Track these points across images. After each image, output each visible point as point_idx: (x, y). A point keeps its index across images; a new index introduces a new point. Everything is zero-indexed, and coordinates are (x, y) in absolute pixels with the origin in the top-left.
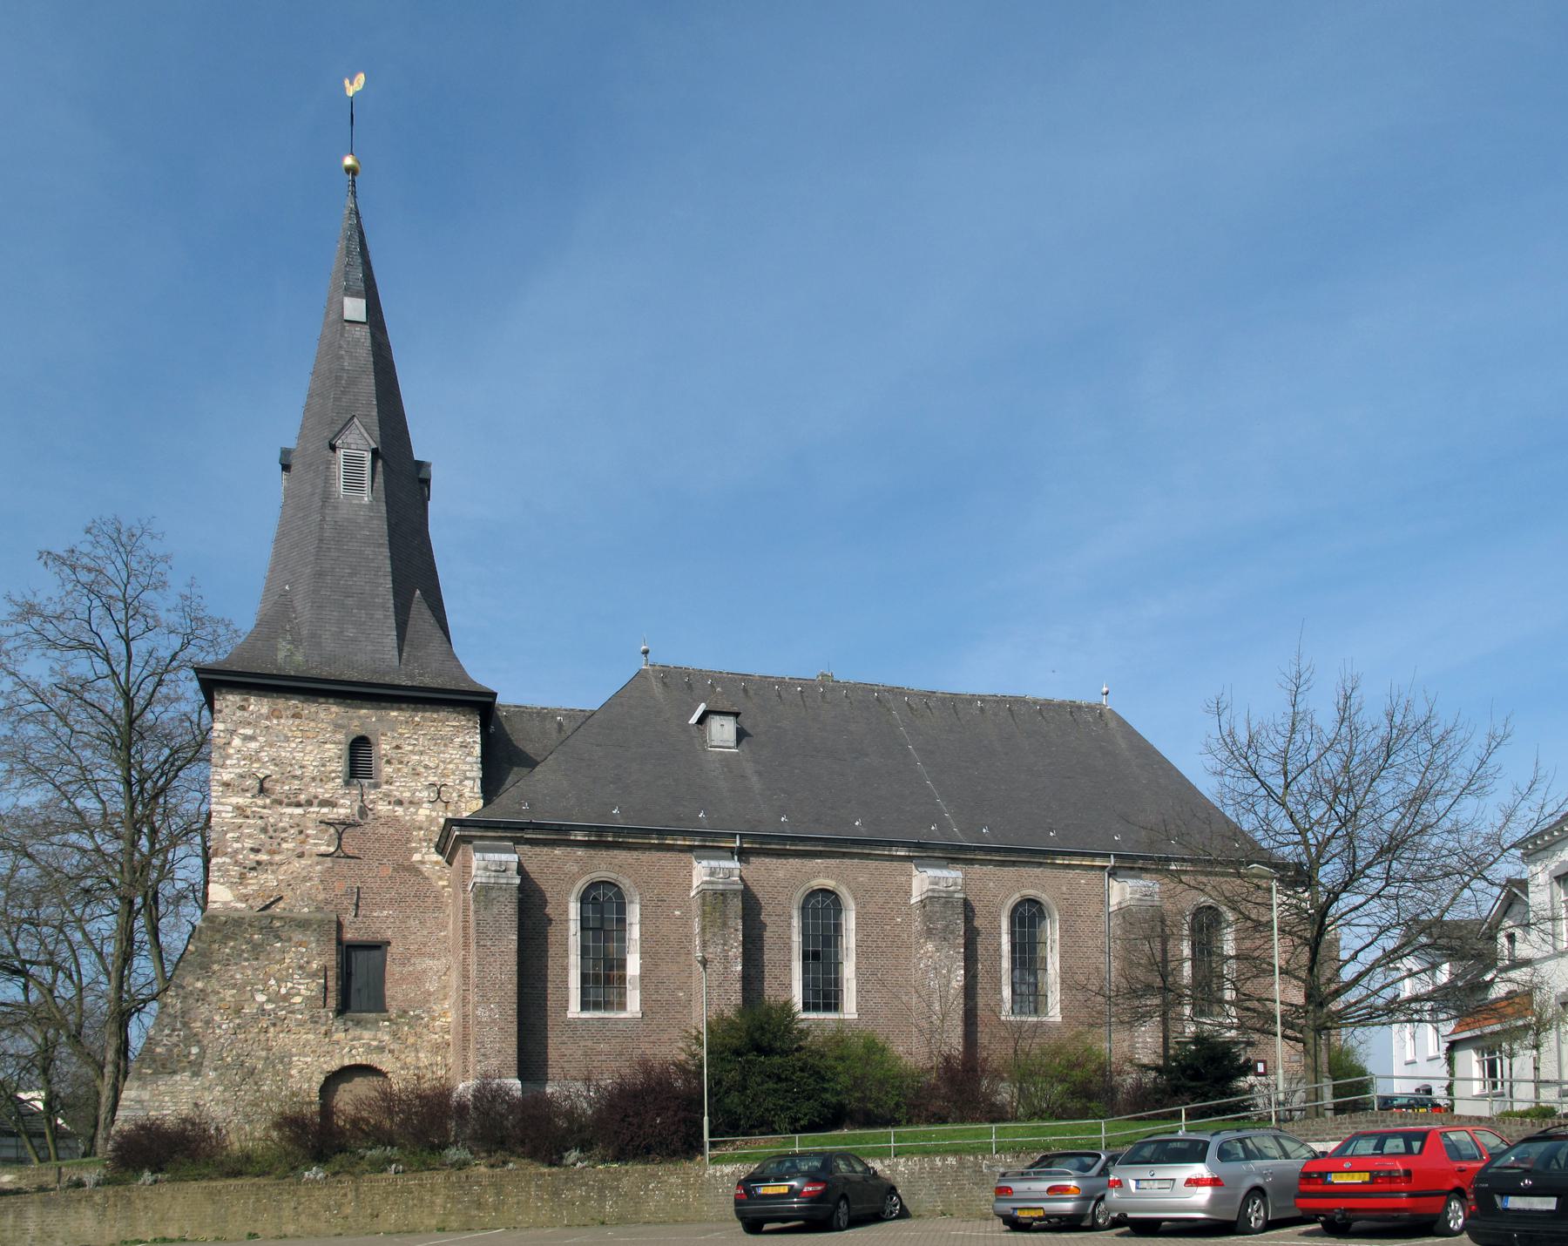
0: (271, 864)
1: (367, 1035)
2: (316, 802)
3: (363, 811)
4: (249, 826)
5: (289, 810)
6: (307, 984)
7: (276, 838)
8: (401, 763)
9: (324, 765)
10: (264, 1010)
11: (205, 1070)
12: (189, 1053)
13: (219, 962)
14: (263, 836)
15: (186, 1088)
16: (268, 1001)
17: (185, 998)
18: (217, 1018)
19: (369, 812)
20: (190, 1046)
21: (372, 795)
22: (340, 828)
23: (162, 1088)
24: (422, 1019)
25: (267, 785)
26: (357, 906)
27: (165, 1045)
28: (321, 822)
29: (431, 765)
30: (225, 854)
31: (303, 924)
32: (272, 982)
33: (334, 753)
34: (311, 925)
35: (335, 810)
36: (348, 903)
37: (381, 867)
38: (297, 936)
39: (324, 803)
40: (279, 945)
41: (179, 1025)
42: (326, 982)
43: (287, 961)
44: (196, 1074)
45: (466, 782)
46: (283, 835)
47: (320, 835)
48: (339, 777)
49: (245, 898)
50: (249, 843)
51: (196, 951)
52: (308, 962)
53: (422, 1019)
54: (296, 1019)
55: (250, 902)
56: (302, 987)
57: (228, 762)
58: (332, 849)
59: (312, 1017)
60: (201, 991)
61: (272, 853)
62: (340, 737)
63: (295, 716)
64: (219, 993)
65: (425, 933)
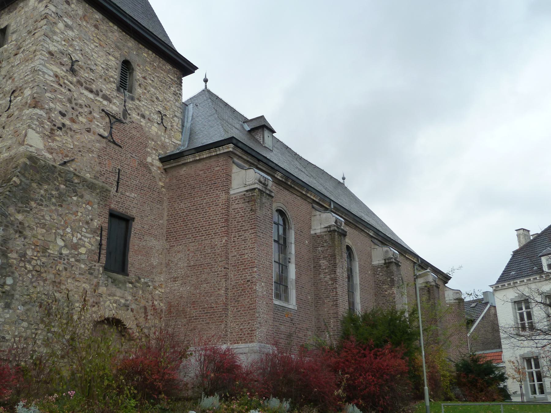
0: (71, 129)
1: (119, 292)
2: (101, 94)
3: (125, 113)
4: (61, 94)
5: (86, 93)
6: (90, 238)
7: (77, 110)
8: (146, 89)
9: (107, 70)
10: (61, 254)
11: (15, 304)
12: (5, 283)
13: (35, 200)
14: (68, 105)
16: (65, 246)
17: (7, 226)
18: (29, 253)
19: (128, 115)
20: (6, 276)
21: (130, 104)
22: (113, 120)
25: (75, 67)
26: (118, 183)
28: (103, 110)
29: (160, 98)
30: (42, 108)
31: (91, 187)
32: (68, 230)
33: (114, 63)
34: (95, 189)
35: (111, 105)
36: (113, 179)
38: (87, 197)
39: (105, 97)
40: (75, 198)
42: (101, 240)
43: (79, 214)
45: (175, 118)
46: (80, 110)
48: (114, 82)
49: (50, 150)
50: (59, 107)
51: (20, 184)
52: (92, 220)
53: (149, 286)
54: (80, 268)
55: (54, 155)
56: (86, 240)
57: (55, 37)
58: (106, 134)
59: (91, 268)
60: (20, 223)
61: (73, 121)
62: (117, 54)
63: (96, 27)
64: (34, 229)
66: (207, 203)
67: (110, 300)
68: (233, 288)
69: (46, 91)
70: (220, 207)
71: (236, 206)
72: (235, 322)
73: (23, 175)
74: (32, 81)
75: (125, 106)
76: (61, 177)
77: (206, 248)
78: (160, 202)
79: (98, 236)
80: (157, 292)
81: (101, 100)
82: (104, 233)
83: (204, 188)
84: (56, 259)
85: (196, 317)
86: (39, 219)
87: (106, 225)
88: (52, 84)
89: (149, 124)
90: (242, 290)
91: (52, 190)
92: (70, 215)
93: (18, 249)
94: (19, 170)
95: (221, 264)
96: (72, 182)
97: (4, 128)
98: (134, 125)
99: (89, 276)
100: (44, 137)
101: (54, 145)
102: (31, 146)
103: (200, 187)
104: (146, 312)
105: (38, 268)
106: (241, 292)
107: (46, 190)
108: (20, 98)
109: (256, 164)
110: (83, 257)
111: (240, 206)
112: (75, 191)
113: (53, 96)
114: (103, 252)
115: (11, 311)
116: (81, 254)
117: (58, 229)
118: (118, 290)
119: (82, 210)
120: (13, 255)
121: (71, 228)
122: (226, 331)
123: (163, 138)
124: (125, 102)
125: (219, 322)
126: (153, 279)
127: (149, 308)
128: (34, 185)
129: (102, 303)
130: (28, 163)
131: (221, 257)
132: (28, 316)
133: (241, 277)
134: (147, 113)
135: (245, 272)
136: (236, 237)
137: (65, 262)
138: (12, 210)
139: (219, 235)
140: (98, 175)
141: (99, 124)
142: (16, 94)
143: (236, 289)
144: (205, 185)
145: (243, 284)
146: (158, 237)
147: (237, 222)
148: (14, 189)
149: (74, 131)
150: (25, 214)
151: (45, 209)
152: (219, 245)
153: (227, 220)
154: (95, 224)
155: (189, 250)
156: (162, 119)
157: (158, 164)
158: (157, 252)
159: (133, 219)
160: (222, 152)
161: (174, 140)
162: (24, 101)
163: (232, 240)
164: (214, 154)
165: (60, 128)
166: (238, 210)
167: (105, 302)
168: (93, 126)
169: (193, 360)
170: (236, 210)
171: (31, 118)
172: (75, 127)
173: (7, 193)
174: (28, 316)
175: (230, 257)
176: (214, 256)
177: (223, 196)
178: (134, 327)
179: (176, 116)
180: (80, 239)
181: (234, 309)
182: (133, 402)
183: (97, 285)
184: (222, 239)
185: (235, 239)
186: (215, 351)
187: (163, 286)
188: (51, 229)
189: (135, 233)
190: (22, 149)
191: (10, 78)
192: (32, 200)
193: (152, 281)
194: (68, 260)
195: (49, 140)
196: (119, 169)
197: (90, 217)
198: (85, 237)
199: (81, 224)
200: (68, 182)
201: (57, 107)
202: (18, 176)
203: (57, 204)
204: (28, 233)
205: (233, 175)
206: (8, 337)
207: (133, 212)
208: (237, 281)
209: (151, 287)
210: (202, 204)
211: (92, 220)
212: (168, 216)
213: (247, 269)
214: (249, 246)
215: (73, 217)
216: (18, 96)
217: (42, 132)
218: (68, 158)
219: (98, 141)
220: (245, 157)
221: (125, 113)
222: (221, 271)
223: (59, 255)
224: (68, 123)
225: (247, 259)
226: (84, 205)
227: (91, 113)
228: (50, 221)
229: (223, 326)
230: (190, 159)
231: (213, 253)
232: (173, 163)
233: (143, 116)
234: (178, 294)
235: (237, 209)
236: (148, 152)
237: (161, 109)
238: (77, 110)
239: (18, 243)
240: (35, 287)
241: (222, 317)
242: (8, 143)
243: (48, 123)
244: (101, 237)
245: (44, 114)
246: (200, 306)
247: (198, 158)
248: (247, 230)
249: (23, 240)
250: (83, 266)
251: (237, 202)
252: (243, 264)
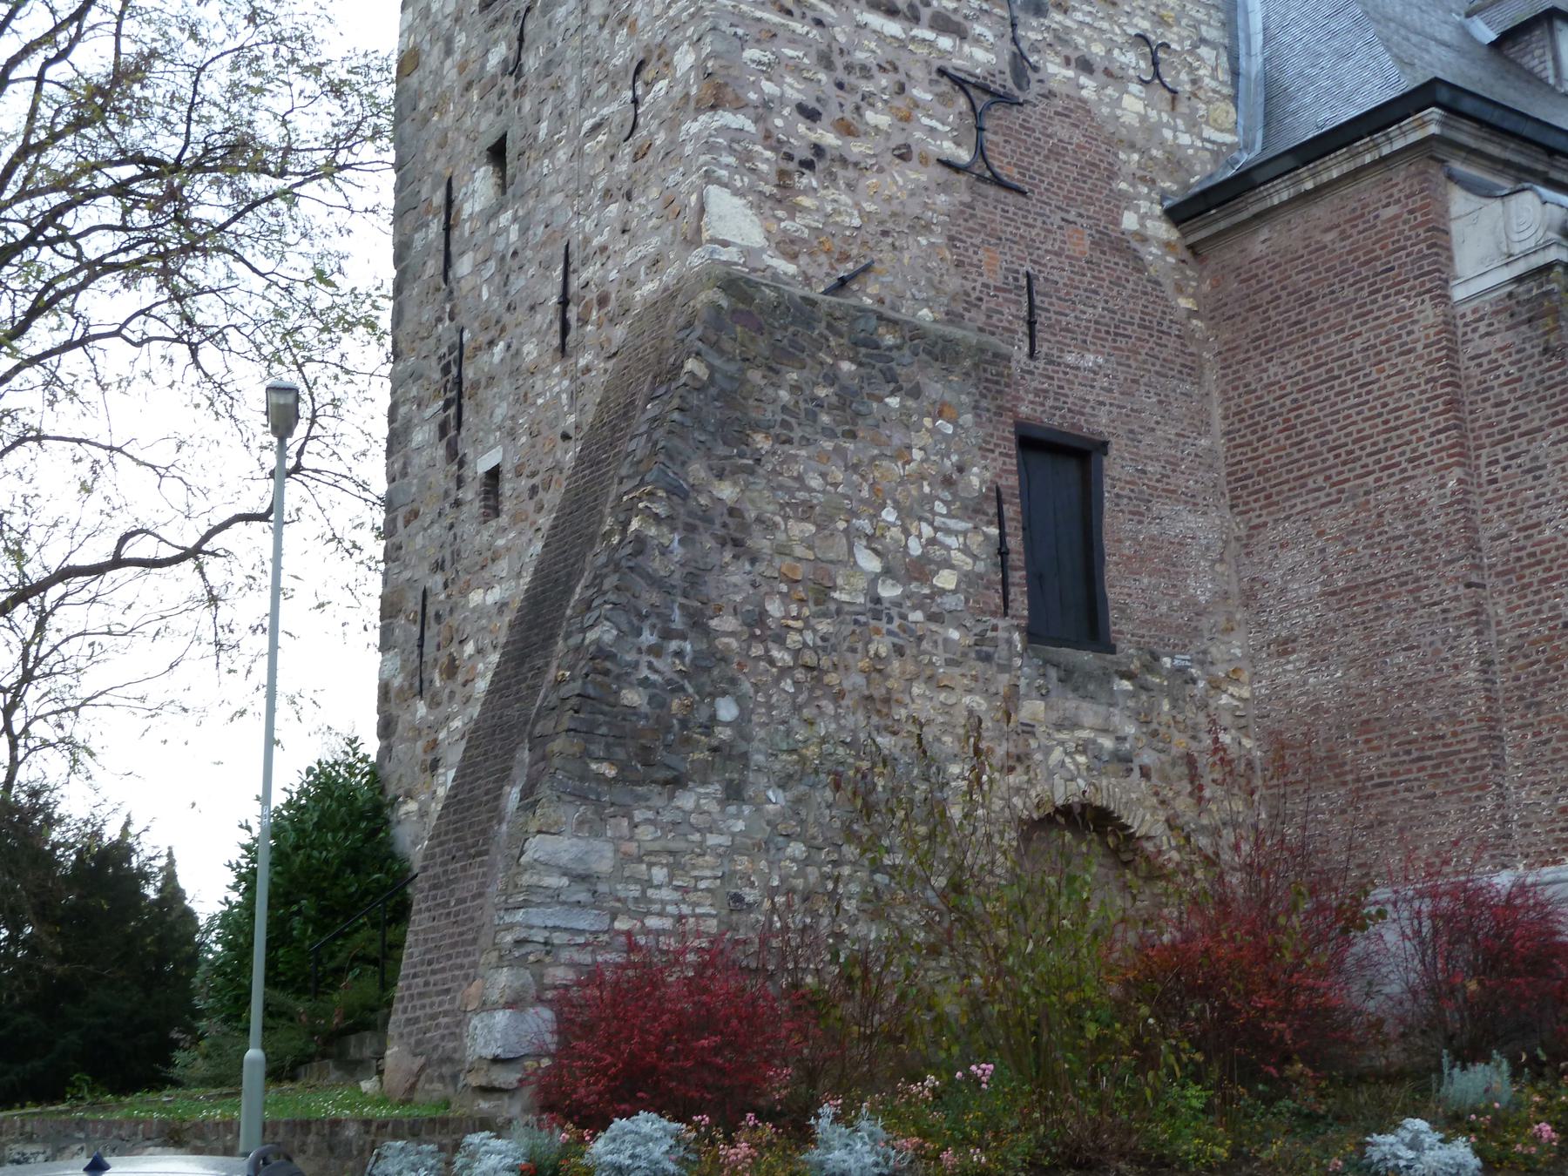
0: (844, 161)
1: (1090, 714)
2: (926, 13)
4: (794, 40)
6: (965, 533)
10: (878, 600)
11: (757, 783)
12: (713, 718)
13: (766, 428)
14: (822, 76)
15: (712, 840)
16: (887, 572)
17: (691, 528)
18: (774, 608)
19: (1030, 73)
20: (713, 696)
22: (982, 100)
23: (646, 833)
24: (1194, 681)
26: (1031, 324)
27: (645, 683)
28: (942, 72)
30: (740, 106)
31: (941, 352)
32: (889, 515)
35: (966, 48)
36: (1012, 312)
37: (1069, 229)
38: (935, 389)
40: (893, 402)
41: (678, 621)
42: (1002, 535)
43: (917, 455)
44: (734, 793)
45: (1204, 51)
46: (866, 87)
47: (940, 109)
49: (788, 247)
50: (794, 90)
52: (961, 469)
53: (1194, 681)
54: (946, 640)
55: (803, 260)
56: (952, 541)
58: (964, 156)
59: (981, 639)
60: (732, 512)
61: (846, 129)
64: (776, 525)
65: (1172, 433)
66: (1366, 349)
67: (1062, 743)
68: (1511, 659)
69: (743, 42)
70: (1420, 357)
71: (1485, 345)
72: (1534, 784)
73: (715, 346)
74: (692, 16)
75: (1015, 41)
76: (839, 334)
77: (1388, 517)
78: (1192, 370)
79: (990, 523)
80: (1224, 699)
81: (929, 35)
82: (1010, 511)
83: (1349, 293)
84: (862, 619)
85: (1380, 776)
86: (790, 491)
87: (1012, 481)
88: (758, 14)
89: (1110, 91)
90: (1548, 661)
91: (815, 384)
92: (885, 463)
93: (738, 598)
94: (699, 332)
95: (1450, 571)
96: (877, 347)
98: (1059, 103)
99: (980, 665)
100: (761, 203)
101: (795, 225)
102: (725, 244)
103: (1333, 292)
104: (1193, 777)
105: (809, 658)
106: (1544, 671)
107: (795, 389)
108: (662, 84)
109: (1540, 167)
110: (950, 602)
111: (1499, 341)
112: (890, 377)
113: (767, 57)
114: (1017, 576)
115: (747, 810)
116: (943, 592)
117: (854, 514)
118: (1085, 705)
119: (926, 439)
120: (725, 623)
121: (897, 506)
122: (1505, 820)
123: (1168, 134)
124: (1014, 26)
125: (1471, 789)
126: (1205, 652)
127: (1203, 761)
128: (755, 376)
129: (1038, 757)
130: (724, 303)
131: (1449, 544)
132: (802, 822)
133: (1538, 612)
134: (1098, 49)
135: (1549, 593)
136: (1497, 462)
137: (894, 626)
138: (697, 470)
139: (1430, 463)
140: (959, 307)
141: (934, 123)
142: (648, 74)
143: (1521, 661)
144: (1351, 280)
145: (1550, 639)
146: (1199, 500)
147: (1497, 405)
148: (694, 400)
149: (856, 164)
150: (742, 478)
151: (803, 453)
153: (1453, 404)
154: (975, 481)
155: (1321, 534)
156: (1155, 63)
157: (1163, 230)
158: (1203, 556)
159: (1103, 447)
160: (1399, 144)
161: (1208, 132)
162: (678, 91)
163: (1485, 477)
164: (1368, 159)
165: (808, 165)
166: (1493, 356)
167: (1048, 751)
168: (918, 135)
169: (1391, 937)
170: (1485, 360)
171: (710, 148)
172: (857, 148)
173: (676, 416)
174: (802, 822)
175: (1484, 543)
176: (1418, 546)
177: (1428, 314)
178: (1159, 829)
179: (1203, 41)
180: (932, 541)
181: (1524, 737)
182: (1195, 1096)
183: (1012, 698)
184: (1442, 477)
185: (1496, 469)
186: (1472, 898)
187: (1245, 677)
188: (832, 519)
189: (1118, 496)
190: (696, 258)
191: (621, 22)
192: (757, 427)
193: (1202, 663)
194: (904, 617)
195: (780, 213)
196: (1028, 275)
197: (955, 458)
198: (949, 532)
199: (927, 489)
200: (865, 347)
201: (789, 92)
202: (698, 354)
203: (839, 430)
204: (760, 542)
205: (1455, 228)
206: (750, 895)
207: (1100, 422)
208: (1525, 630)
209: (1201, 684)
210: (1350, 355)
211: (961, 469)
212: (1226, 418)
213: (1557, 578)
214: (1554, 492)
215: (898, 469)
216: (655, 80)
217: (751, 189)
218: (850, 266)
219: (944, 187)
220: (1493, 149)
221: (1021, 65)
222: (1457, 599)
223: (869, 605)
224: (830, 139)
225: (1555, 539)
226: (927, 422)
227: (901, 89)
228: (824, 492)
229: (1489, 803)
230: (1281, 193)
231: (1417, 534)
232: (1216, 221)
233: (1085, 66)
234: (1303, 699)
235: (1489, 353)
236: (1121, 193)
237: (1145, 25)
238: (854, 90)
239: (735, 579)
240: (810, 723)
241: (1481, 768)
242: (651, 245)
243: (768, 154)
244: (1001, 526)
245: (750, 126)
246: (1392, 736)
247: (1309, 185)
248: (1540, 429)
249: (748, 567)
250: (955, 634)
251: (1483, 330)
252: (1539, 563)
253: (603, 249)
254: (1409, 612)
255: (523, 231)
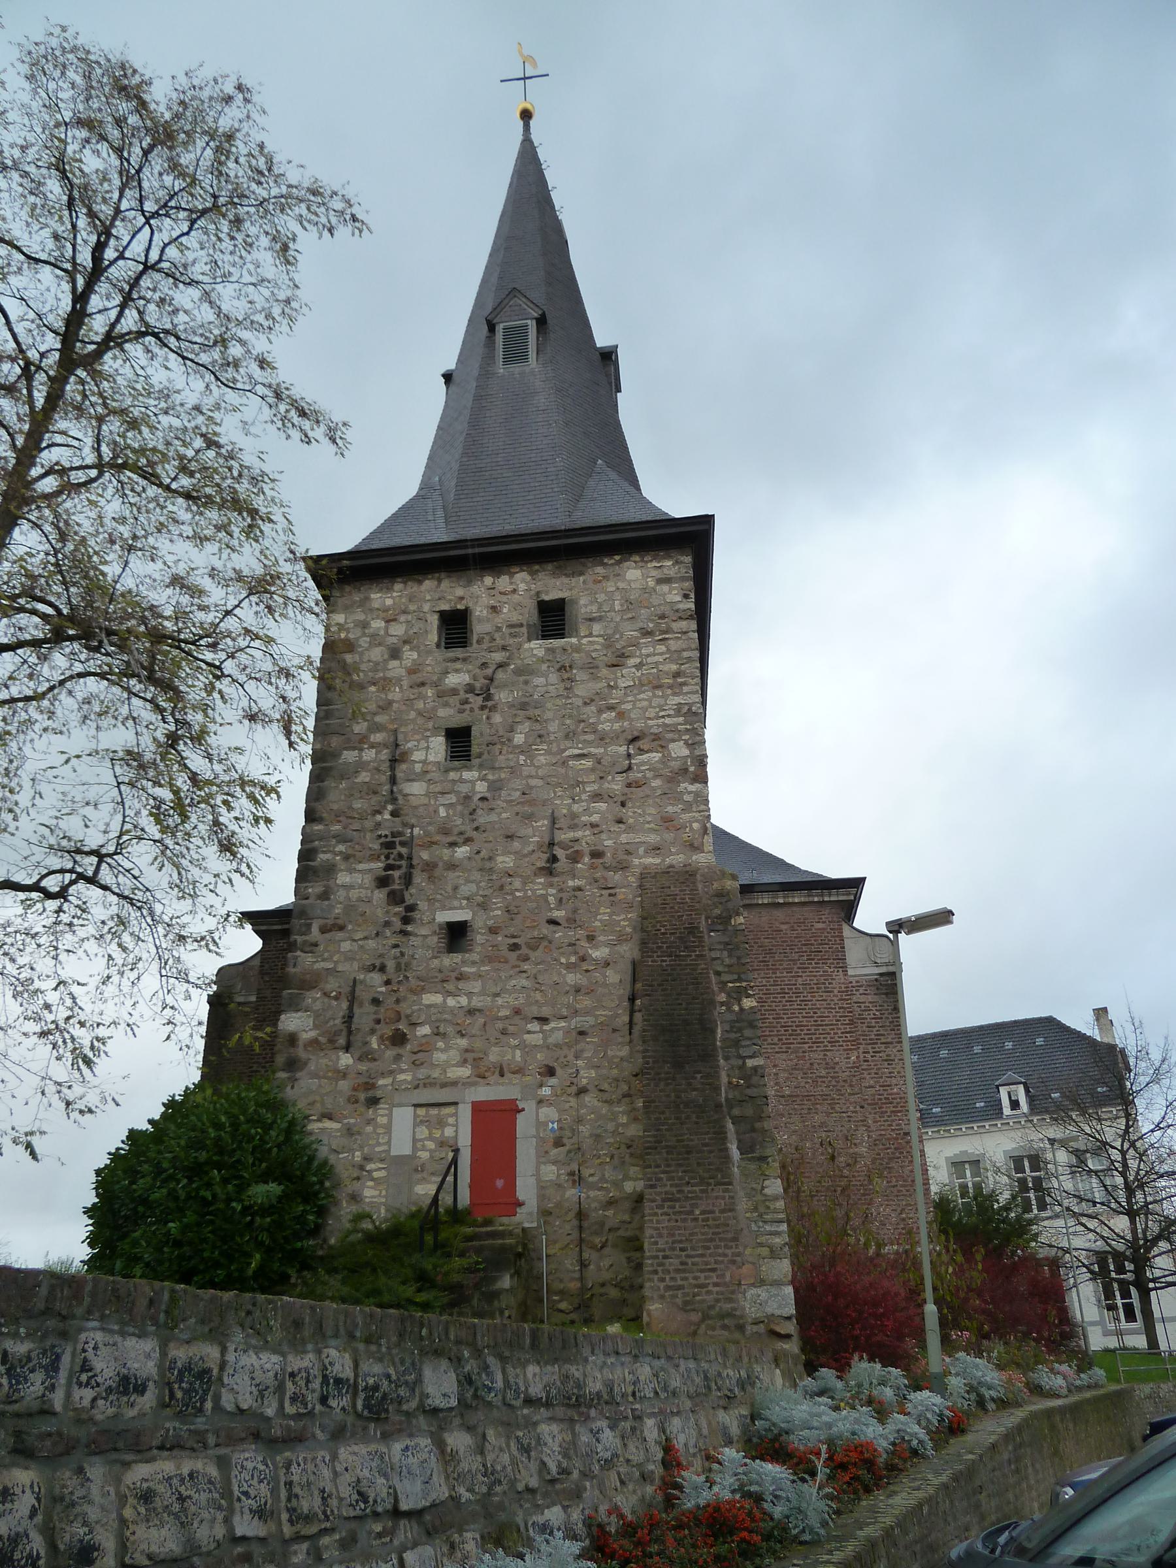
77: (816, 1066)
83: (796, 956)
97: (623, 804)
111: (870, 998)
131: (851, 1086)
142: (643, 744)
152: (843, 1065)
155: (775, 1066)
160: (833, 899)
164: (816, 899)
176: (834, 1083)
191: (611, 708)
222: (856, 1112)
230: (765, 899)
242: (653, 838)
247: (781, 901)
253: (593, 825)
254: (828, 1114)
255: (495, 787)
